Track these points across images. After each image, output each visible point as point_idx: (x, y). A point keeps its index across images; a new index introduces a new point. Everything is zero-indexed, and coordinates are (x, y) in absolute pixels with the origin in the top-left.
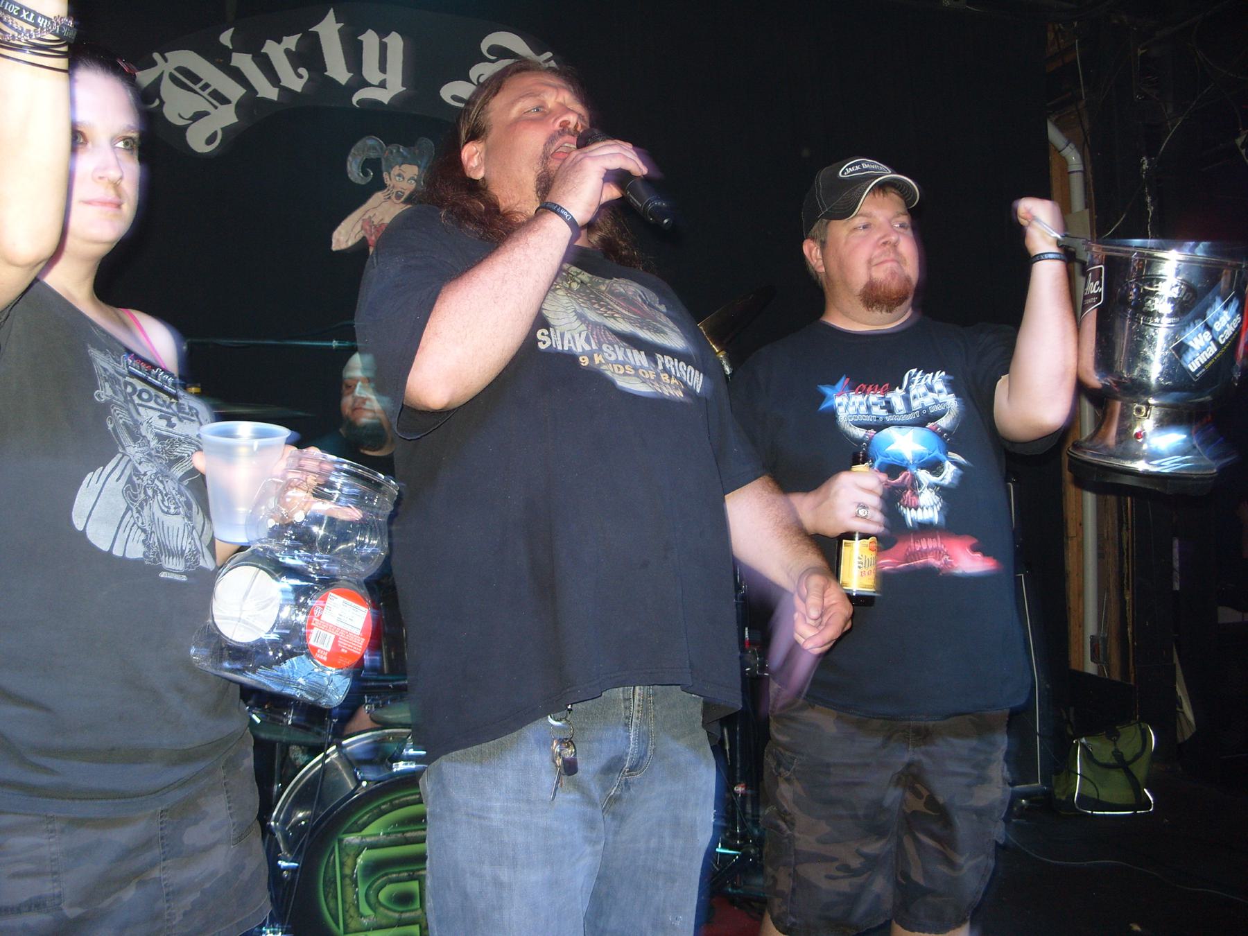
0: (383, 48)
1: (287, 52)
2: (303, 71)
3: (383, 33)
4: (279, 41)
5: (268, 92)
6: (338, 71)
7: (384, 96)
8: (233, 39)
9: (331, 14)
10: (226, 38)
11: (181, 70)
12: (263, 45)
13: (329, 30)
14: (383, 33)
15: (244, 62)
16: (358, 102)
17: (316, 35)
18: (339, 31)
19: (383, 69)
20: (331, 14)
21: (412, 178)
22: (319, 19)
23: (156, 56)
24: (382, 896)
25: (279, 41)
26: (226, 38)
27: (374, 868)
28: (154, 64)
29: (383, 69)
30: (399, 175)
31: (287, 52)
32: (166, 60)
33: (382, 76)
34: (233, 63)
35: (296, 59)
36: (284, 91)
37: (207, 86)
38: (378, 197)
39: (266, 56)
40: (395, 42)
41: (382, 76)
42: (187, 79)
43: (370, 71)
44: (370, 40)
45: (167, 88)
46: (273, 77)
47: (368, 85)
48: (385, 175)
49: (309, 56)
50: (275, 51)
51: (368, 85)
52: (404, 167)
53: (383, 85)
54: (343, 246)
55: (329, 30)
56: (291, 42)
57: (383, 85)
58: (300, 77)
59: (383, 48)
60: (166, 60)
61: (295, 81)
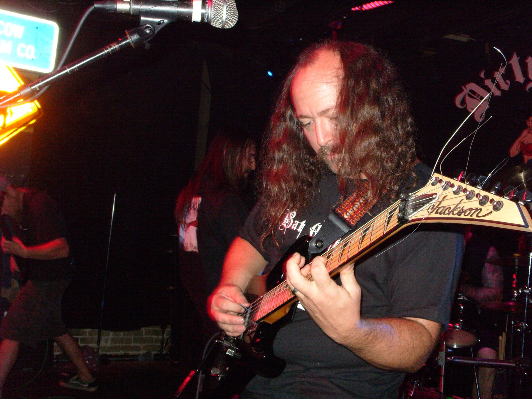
2: (508, 81)
5: (498, 93)
6: (520, 78)
8: (485, 75)
10: (482, 75)
11: (471, 91)
15: (488, 82)
16: (529, 90)
18: (519, 61)
23: (463, 88)
26: (482, 75)
28: (462, 91)
31: (503, 75)
32: (466, 88)
34: (486, 84)
36: (503, 91)
37: (479, 95)
38: (525, 132)
42: (473, 94)
45: (468, 99)
46: (498, 86)
48: (527, 122)
49: (509, 75)
50: (498, 76)
54: (515, 155)
58: (507, 84)
60: (466, 88)
61: (505, 87)
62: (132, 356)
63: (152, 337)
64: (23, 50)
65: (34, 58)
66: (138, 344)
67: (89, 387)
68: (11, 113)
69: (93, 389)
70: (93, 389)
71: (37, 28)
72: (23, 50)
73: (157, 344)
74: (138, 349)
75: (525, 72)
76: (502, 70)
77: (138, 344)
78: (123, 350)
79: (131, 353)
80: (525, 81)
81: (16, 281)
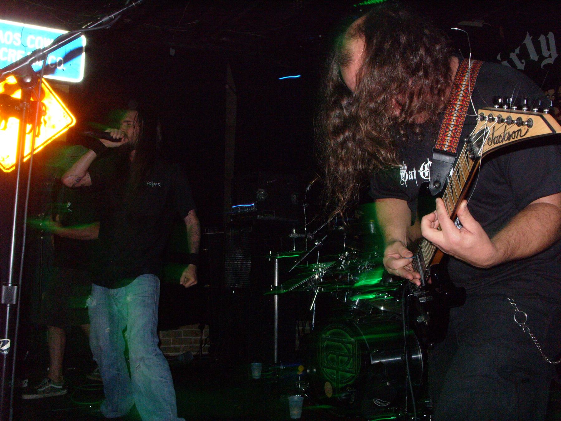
0: (547, 40)
1: (517, 55)
2: (523, 61)
3: (546, 34)
4: (514, 52)
6: (534, 56)
7: (551, 61)
9: (528, 35)
10: (499, 57)
12: (509, 55)
13: (528, 41)
14: (546, 34)
16: (544, 66)
17: (525, 44)
19: (549, 49)
20: (528, 35)
21: (553, 95)
22: (524, 38)
24: (329, 357)
25: (514, 52)
26: (499, 57)
27: (328, 347)
29: (549, 49)
30: (548, 95)
31: (517, 55)
33: (549, 53)
35: (520, 57)
39: (511, 59)
40: (551, 35)
41: (549, 53)
43: (545, 53)
44: (542, 39)
47: (545, 58)
49: (524, 55)
50: (513, 56)
51: (545, 58)
52: (549, 91)
53: (550, 56)
55: (528, 41)
56: (517, 51)
57: (550, 56)
58: (523, 63)
59: (547, 40)
68: (45, 122)
75: (538, 50)
76: (517, 51)
80: (539, 59)
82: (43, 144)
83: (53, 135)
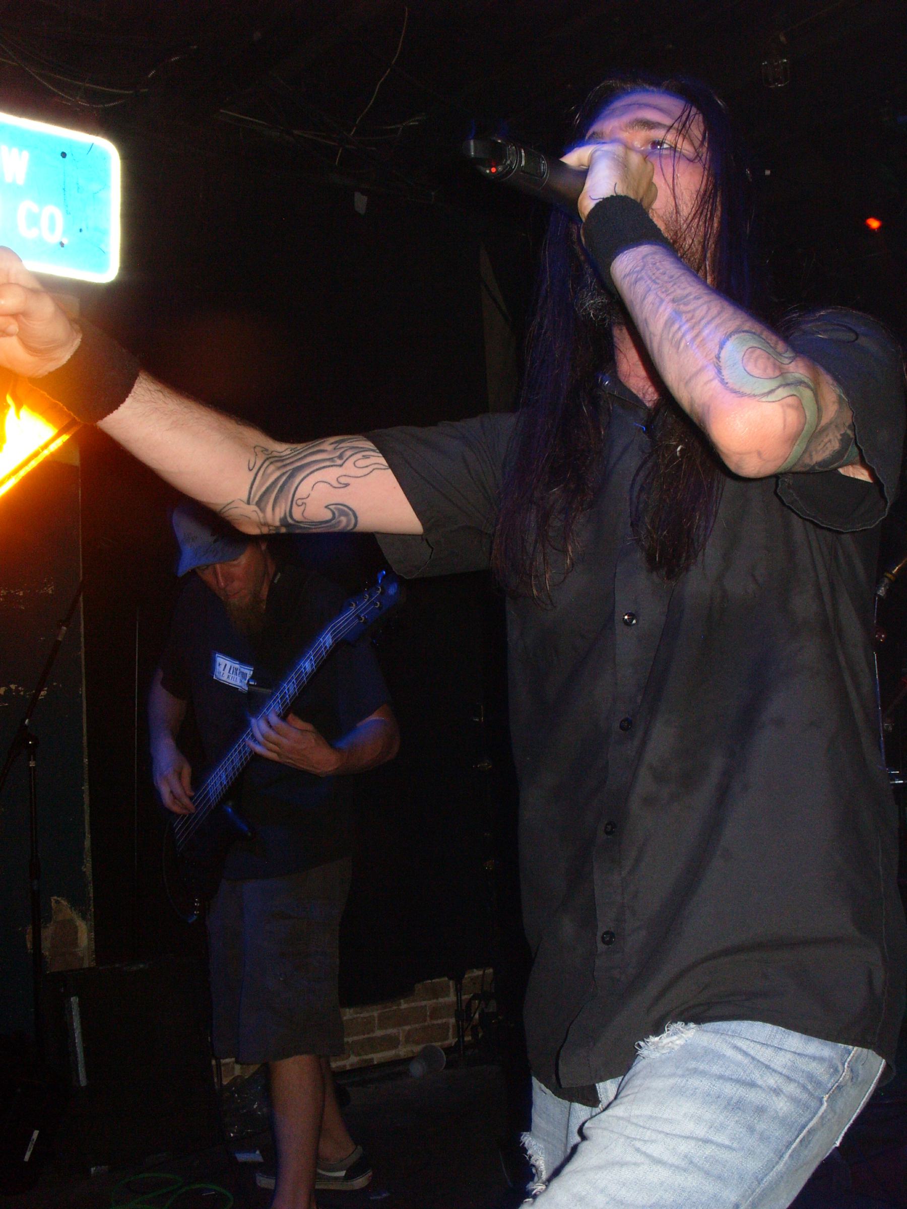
62: (381, 1065)
63: (424, 1003)
64: (33, 220)
65: (65, 242)
66: (391, 1031)
67: (349, 1177)
69: (360, 1182)
70: (360, 1182)
71: (64, 155)
72: (33, 220)
73: (435, 1022)
74: (392, 1042)
77: (391, 1031)
78: (357, 1054)
79: (377, 1057)
81: (64, 903)
82: (15, 472)
83: (42, 443)
